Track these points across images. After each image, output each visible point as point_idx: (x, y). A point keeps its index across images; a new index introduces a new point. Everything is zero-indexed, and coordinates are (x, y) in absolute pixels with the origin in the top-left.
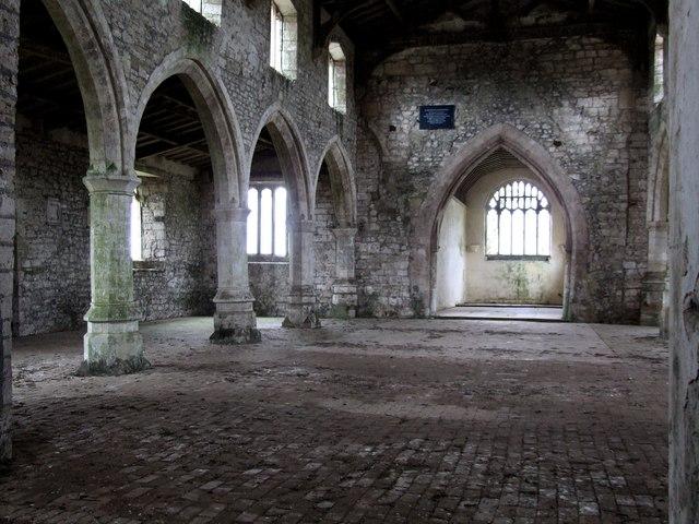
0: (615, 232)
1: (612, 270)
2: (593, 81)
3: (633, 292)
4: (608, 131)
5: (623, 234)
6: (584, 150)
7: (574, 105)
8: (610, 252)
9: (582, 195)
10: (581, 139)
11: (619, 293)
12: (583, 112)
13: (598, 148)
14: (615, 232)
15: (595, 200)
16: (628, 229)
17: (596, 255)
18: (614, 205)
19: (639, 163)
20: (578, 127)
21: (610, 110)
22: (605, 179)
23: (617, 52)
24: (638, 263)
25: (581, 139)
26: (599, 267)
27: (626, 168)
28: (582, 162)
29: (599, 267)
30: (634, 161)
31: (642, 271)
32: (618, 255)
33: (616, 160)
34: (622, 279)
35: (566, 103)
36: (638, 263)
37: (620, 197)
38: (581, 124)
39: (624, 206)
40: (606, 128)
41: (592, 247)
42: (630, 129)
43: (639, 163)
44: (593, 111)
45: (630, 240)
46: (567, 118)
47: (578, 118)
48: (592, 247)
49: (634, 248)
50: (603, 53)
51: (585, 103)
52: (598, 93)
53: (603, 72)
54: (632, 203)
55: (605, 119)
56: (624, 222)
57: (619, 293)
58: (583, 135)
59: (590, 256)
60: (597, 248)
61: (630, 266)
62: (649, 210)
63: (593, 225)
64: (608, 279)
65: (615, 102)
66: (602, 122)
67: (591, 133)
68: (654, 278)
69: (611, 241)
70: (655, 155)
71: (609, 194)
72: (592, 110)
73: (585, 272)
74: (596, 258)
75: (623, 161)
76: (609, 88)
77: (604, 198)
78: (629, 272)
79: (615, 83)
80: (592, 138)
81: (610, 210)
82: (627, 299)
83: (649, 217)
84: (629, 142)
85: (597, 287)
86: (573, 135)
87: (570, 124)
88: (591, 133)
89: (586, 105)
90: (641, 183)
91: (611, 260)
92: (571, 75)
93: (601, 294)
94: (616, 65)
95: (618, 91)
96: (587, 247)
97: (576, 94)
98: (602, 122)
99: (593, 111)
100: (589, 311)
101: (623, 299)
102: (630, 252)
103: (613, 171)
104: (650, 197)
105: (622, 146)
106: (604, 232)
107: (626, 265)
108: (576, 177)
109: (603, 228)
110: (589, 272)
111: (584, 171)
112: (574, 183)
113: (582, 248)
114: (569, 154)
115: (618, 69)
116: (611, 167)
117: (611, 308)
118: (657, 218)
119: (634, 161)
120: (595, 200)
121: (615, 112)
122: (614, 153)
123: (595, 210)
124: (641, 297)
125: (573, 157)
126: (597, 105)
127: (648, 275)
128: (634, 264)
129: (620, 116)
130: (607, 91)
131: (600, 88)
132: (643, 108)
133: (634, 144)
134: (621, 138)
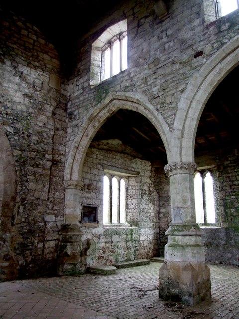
0: (40, 186)
1: (35, 223)
2: (33, 56)
3: (52, 244)
4: (40, 99)
5: (46, 189)
6: (19, 107)
7: (15, 68)
8: (34, 205)
9: (14, 147)
10: (18, 97)
11: (40, 245)
12: (21, 75)
13: (31, 110)
14: (40, 186)
15: (25, 154)
16: (50, 185)
17: (22, 208)
18: (41, 162)
19: (61, 132)
20: (16, 87)
21: (42, 84)
22: (35, 138)
23: (51, 46)
24: (56, 216)
25: (18, 97)
26: (23, 220)
27: (52, 133)
28: (16, 118)
29: (23, 220)
30: (58, 129)
31: (59, 224)
32: (40, 209)
33: (44, 124)
34: (43, 232)
35: (9, 63)
36: (56, 216)
37: (47, 156)
38: (19, 85)
39: (49, 164)
40: (39, 96)
41: (18, 200)
42: (55, 104)
43: (61, 132)
44: (31, 79)
45: (51, 195)
46: (7, 75)
47: (17, 79)
48: (18, 200)
49: (53, 203)
50: (43, 42)
51: (26, 70)
52: (36, 67)
53: (41, 54)
54: (55, 163)
55: (38, 89)
56: (47, 179)
57: (40, 245)
58: (19, 94)
59: (16, 209)
60: (23, 200)
61: (50, 218)
62: (67, 171)
63: (21, 179)
64: (31, 232)
65: (47, 80)
66: (36, 90)
67: (26, 95)
68: (72, 230)
69: (37, 195)
70: (84, 125)
71: (38, 151)
72: (29, 78)
73: (9, 226)
74: (21, 210)
75: (49, 126)
76: (43, 67)
77: (33, 154)
78: (49, 225)
79: (48, 66)
80: (27, 100)
81: (38, 166)
82: (47, 251)
83: (67, 177)
84: (54, 114)
85: (20, 240)
86: (12, 92)
87: (10, 81)
88: (26, 95)
89: (25, 72)
90: (61, 147)
91: (35, 213)
92: (15, 43)
93: (23, 248)
94: (49, 54)
95: (51, 71)
96: (14, 199)
97: (18, 59)
98: (36, 90)
99: (31, 79)
100: (11, 266)
101: (43, 250)
102: (51, 207)
103: (42, 132)
104: (70, 160)
105: (50, 114)
106: (31, 186)
107: (47, 218)
108: (9, 129)
109: (31, 181)
110: (13, 225)
111: (17, 126)
112: (7, 134)
113: (9, 199)
114: (6, 107)
115: (52, 57)
116: (40, 129)
117: (33, 261)
118: (76, 177)
119: (58, 129)
120: (25, 154)
121: (46, 87)
122: (43, 118)
123: (24, 164)
124: (60, 249)
125: (9, 110)
126: (33, 75)
127: (65, 228)
128: (53, 217)
129: (49, 91)
130: (43, 70)
131: (37, 64)
132: (64, 92)
133: (56, 116)
134: (49, 109)
